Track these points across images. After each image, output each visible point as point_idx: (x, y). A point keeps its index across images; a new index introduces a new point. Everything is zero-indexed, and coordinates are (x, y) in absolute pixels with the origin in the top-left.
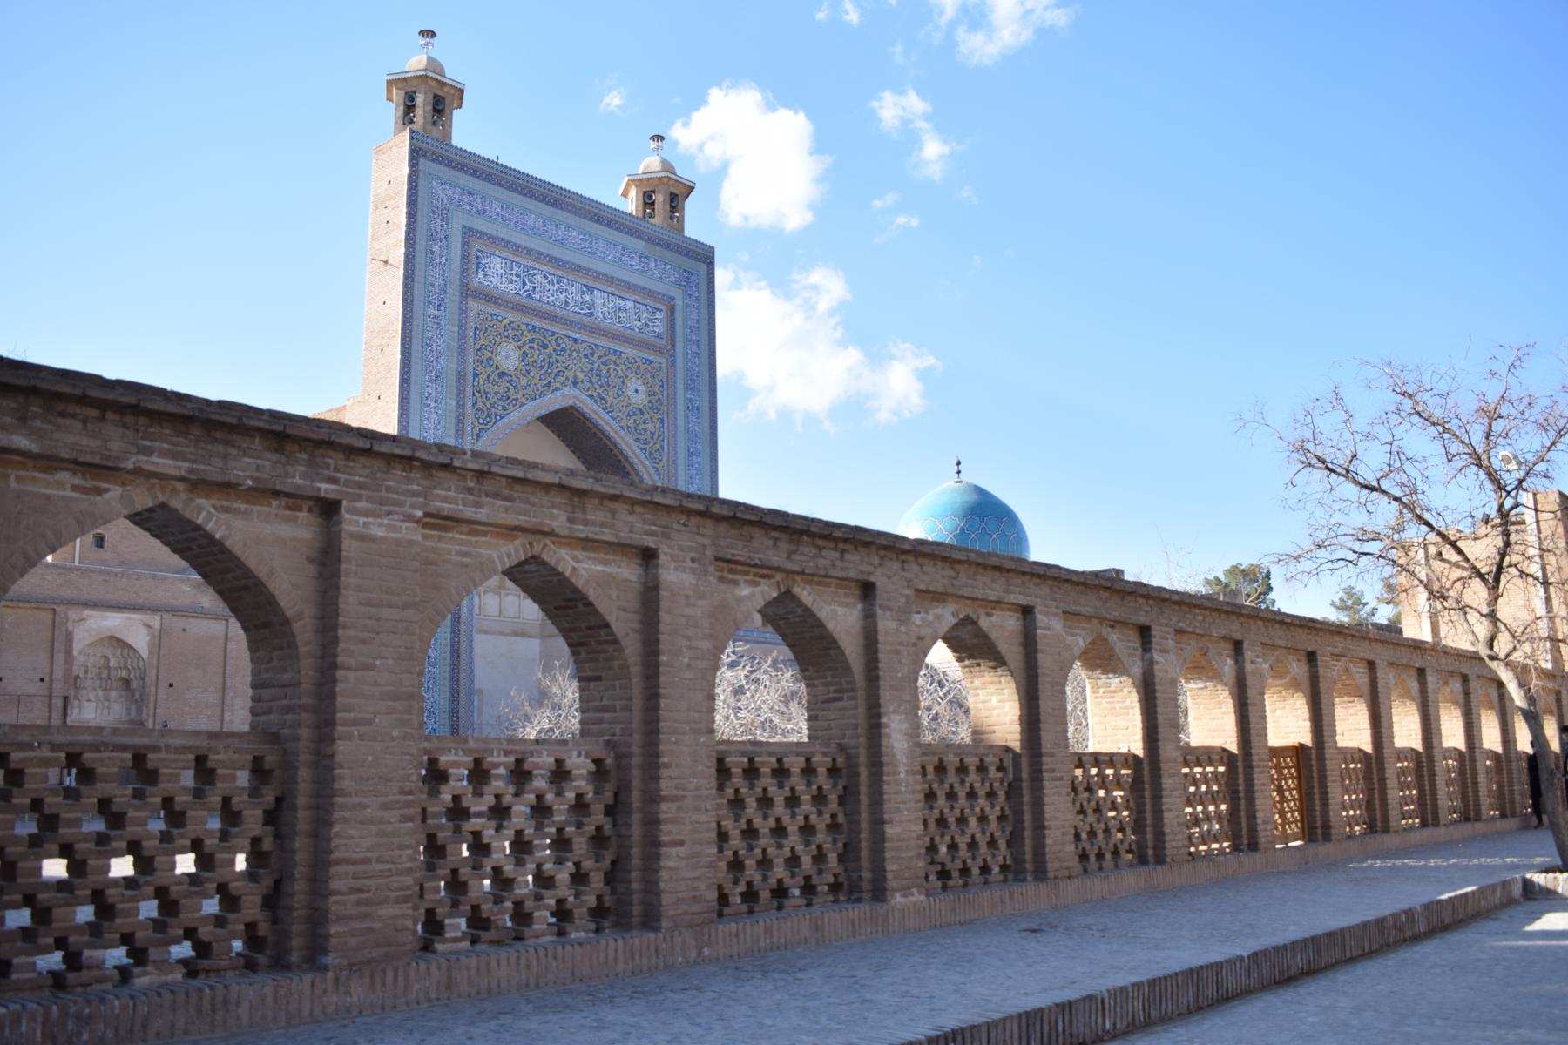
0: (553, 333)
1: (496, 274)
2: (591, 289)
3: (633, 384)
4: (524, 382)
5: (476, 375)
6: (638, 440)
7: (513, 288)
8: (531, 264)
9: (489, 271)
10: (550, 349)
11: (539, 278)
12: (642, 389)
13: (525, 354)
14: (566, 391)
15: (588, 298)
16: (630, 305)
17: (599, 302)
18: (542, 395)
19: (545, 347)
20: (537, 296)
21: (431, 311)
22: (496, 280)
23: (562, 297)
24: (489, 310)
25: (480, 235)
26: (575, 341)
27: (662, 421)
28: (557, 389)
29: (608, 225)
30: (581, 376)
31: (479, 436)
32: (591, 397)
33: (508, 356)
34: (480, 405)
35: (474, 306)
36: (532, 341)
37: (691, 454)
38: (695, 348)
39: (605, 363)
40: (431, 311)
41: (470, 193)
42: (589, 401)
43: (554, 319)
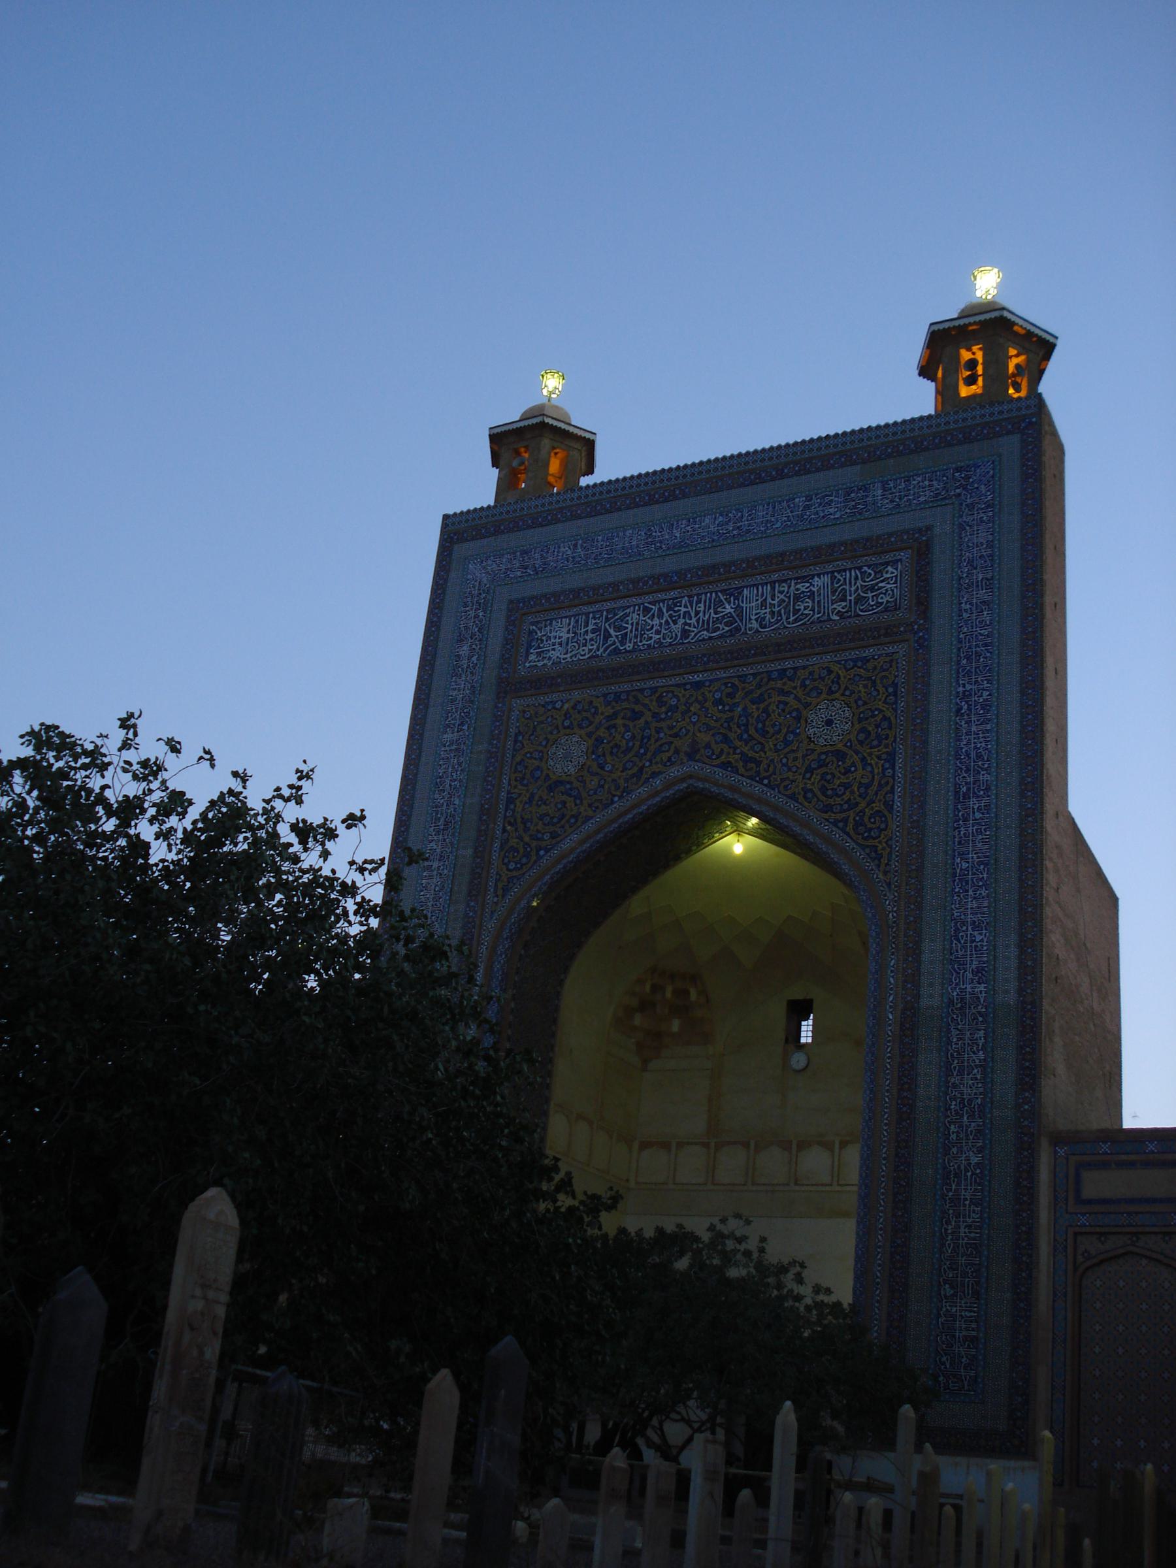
0: (654, 690)
1: (561, 643)
2: (735, 594)
4: (593, 783)
5: (510, 801)
6: (827, 809)
7: (584, 652)
8: (620, 603)
9: (546, 645)
10: (648, 716)
13: (599, 741)
14: (674, 772)
15: (729, 609)
19: (636, 716)
20: (629, 646)
21: (449, 736)
22: (554, 655)
23: (677, 628)
24: (542, 699)
26: (698, 685)
27: (891, 758)
28: (654, 775)
29: (781, 475)
31: (506, 890)
32: (725, 765)
33: (569, 756)
34: (513, 842)
35: (518, 704)
36: (614, 716)
37: (960, 798)
38: (983, 594)
39: (761, 699)
40: (449, 736)
41: (524, 553)
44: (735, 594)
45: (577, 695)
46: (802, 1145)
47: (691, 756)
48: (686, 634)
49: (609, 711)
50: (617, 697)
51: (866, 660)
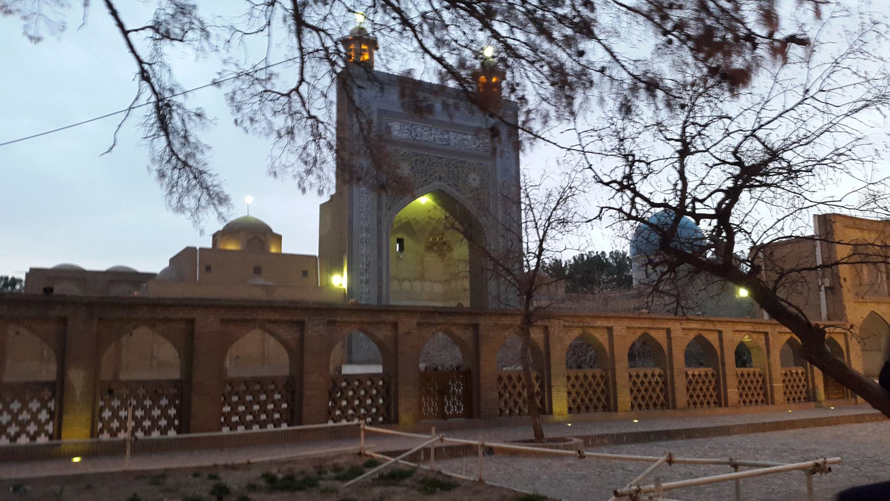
2: (448, 132)
3: (472, 176)
7: (405, 136)
11: (419, 129)
12: (478, 178)
13: (413, 167)
15: (446, 136)
16: (469, 137)
17: (452, 138)
18: (422, 186)
19: (423, 162)
25: (386, 112)
26: (440, 158)
28: (430, 182)
30: (443, 175)
31: (389, 209)
42: (448, 187)
43: (427, 148)
44: (448, 132)
45: (405, 150)
46: (403, 280)
47: (440, 179)
48: (434, 140)
49: (415, 158)
50: (417, 154)
51: (482, 164)
